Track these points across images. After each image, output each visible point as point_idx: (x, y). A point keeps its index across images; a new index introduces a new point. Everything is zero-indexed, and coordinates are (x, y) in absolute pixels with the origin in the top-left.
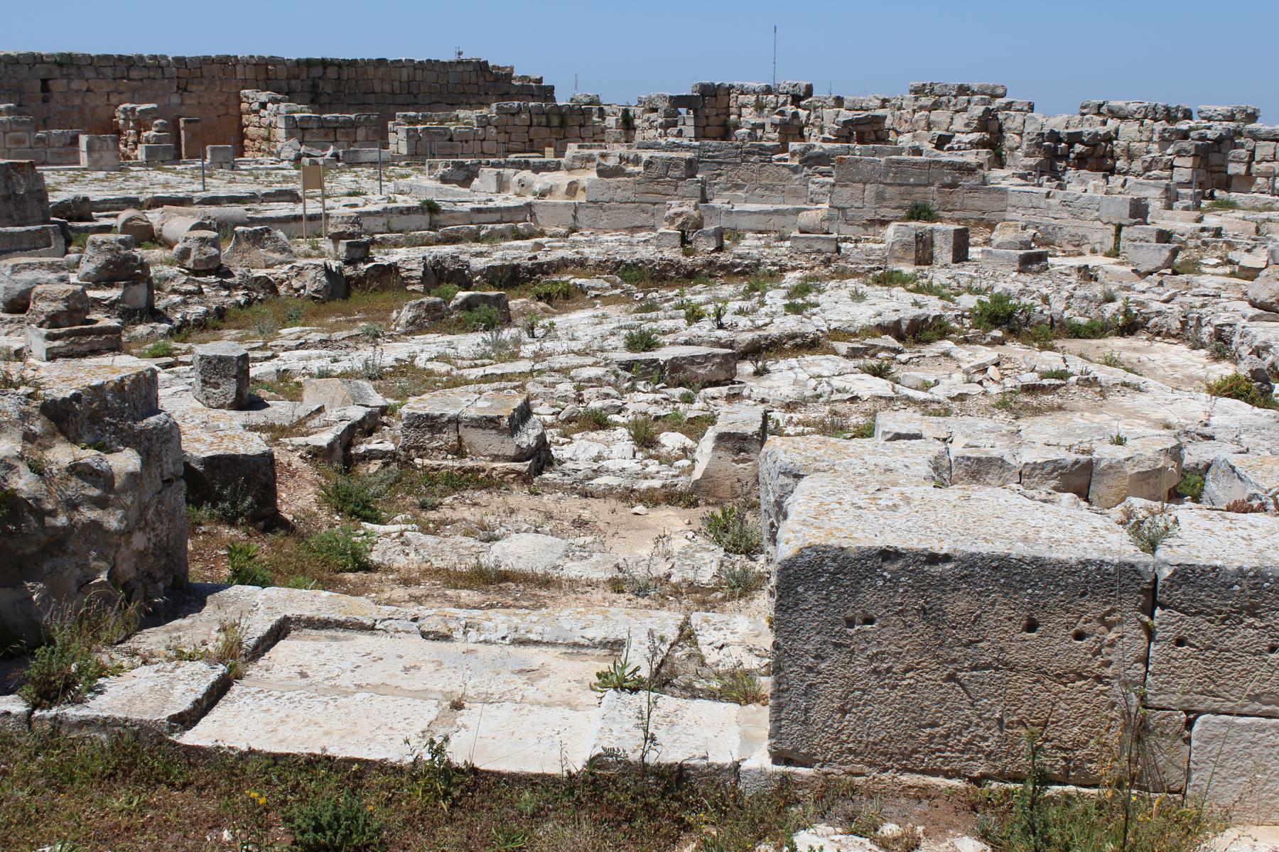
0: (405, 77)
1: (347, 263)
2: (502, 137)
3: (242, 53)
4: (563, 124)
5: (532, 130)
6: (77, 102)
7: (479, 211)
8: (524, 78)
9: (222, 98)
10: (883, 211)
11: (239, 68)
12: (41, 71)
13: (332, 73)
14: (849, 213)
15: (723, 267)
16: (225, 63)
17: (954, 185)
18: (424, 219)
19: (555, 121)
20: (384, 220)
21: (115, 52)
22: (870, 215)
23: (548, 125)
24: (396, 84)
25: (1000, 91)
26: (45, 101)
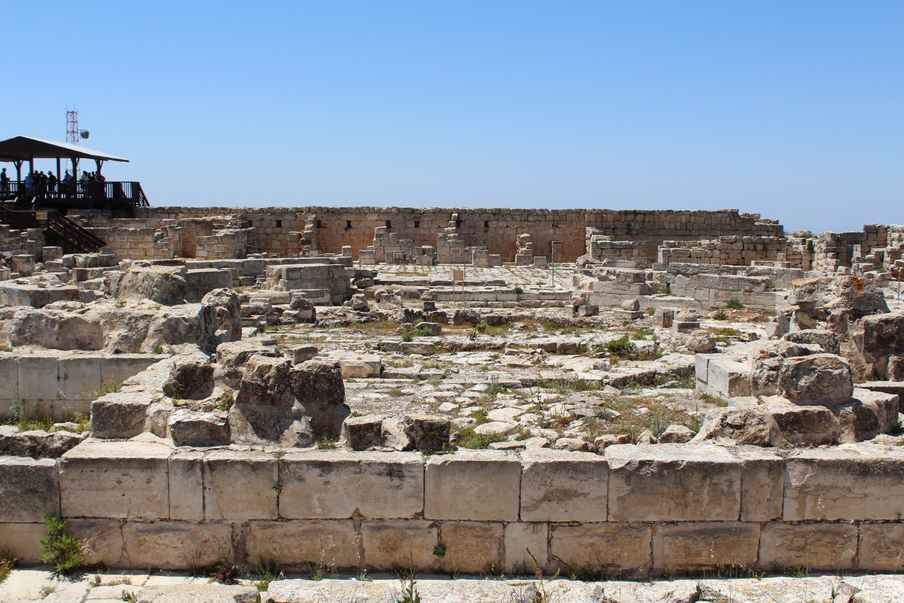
0: (684, 220)
2: (723, 256)
3: (589, 207)
5: (744, 253)
6: (501, 232)
7: (544, 294)
8: (766, 221)
9: (576, 231)
10: (718, 303)
13: (639, 218)
14: (703, 303)
15: (586, 323)
16: (580, 213)
17: (750, 291)
18: (515, 296)
19: (760, 247)
20: (494, 295)
21: (522, 208)
22: (712, 305)
23: (755, 249)
24: (678, 224)
26: (486, 231)
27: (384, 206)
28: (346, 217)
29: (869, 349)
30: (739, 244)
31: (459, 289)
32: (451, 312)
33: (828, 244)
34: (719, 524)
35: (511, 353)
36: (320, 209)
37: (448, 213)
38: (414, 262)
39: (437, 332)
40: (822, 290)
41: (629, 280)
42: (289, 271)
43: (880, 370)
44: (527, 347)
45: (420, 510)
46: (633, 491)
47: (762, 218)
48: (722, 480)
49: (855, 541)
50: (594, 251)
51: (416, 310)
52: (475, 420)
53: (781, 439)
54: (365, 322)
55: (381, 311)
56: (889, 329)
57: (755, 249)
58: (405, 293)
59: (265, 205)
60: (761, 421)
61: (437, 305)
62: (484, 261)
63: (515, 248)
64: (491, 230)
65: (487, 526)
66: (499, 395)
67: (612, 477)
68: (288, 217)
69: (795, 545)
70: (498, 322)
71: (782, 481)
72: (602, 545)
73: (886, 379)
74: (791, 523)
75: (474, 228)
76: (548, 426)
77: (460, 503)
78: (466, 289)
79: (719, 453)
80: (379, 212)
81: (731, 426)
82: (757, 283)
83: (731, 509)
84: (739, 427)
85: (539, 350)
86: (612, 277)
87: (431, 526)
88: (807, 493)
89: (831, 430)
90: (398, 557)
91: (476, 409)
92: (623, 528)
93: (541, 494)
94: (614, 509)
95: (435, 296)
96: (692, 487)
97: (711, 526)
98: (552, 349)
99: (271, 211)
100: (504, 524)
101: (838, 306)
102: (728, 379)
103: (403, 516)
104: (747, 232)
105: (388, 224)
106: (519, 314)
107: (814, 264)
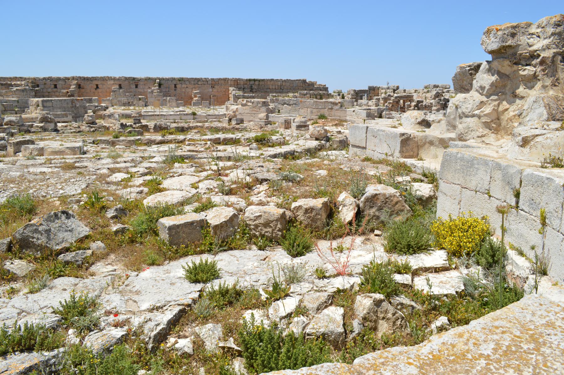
0: (279, 84)
1: (134, 124)
6: (184, 90)
7: (209, 115)
8: (320, 85)
10: (313, 117)
12: (174, 82)
13: (257, 83)
16: (225, 80)
17: (332, 109)
18: (192, 116)
19: (319, 97)
20: (179, 117)
21: (194, 77)
24: (277, 86)
25: (448, 87)
26: (175, 90)
27: (117, 76)
28: (95, 82)
32: (151, 124)
33: (352, 95)
35: (189, 145)
36: (80, 77)
37: (154, 80)
38: (134, 105)
39: (142, 134)
41: (260, 105)
42: (43, 101)
44: (200, 140)
47: (318, 83)
50: (234, 99)
52: (146, 190)
54: (93, 131)
55: (104, 125)
58: (123, 115)
59: (47, 75)
61: (142, 121)
63: (192, 99)
64: (178, 89)
66: (176, 165)
68: (60, 82)
70: (182, 130)
76: (230, 192)
80: (114, 79)
85: (209, 142)
86: (249, 104)
91: (148, 178)
98: (217, 142)
99: (50, 79)
101: (548, 47)
102: (399, 140)
105: (120, 87)
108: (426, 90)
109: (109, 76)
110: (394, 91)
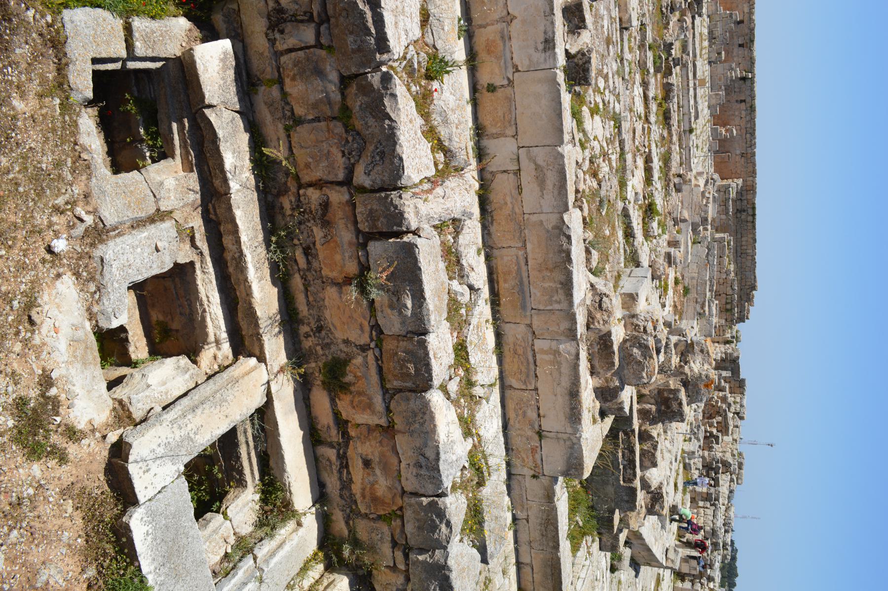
0: (748, 251)
2: (721, 281)
3: (758, 180)
4: (727, 310)
6: (737, 113)
8: (748, 310)
11: (751, 178)
12: (748, 100)
13: (750, 218)
16: (754, 172)
17: (697, 302)
18: (687, 128)
19: (729, 307)
22: (685, 275)
23: (727, 303)
25: (740, 482)
26: (737, 101)
27: (756, 17)
29: (660, 392)
30: (730, 292)
31: (691, 84)
32: (674, 79)
33: (731, 354)
34: (528, 294)
35: (643, 129)
37: (751, 70)
38: (710, 46)
39: (657, 70)
40: (704, 359)
41: (703, 214)
43: (645, 399)
44: (649, 141)
45: (520, 69)
46: (548, 231)
47: (751, 308)
48: (561, 296)
49: (524, 387)
50: (723, 186)
51: (673, 52)
52: (592, 106)
53: (593, 336)
54: (662, 11)
55: (671, 23)
56: (675, 406)
57: (727, 303)
58: (686, 41)
60: (605, 322)
61: (678, 68)
62: (714, 102)
63: (724, 125)
64: (738, 105)
65: (513, 123)
66: (612, 123)
67: (557, 216)
69: (518, 347)
71: (562, 338)
72: (507, 211)
73: (638, 403)
74: (533, 345)
75: (740, 92)
76: (591, 162)
77: (528, 99)
78: (691, 90)
79: (581, 293)
80: (751, 13)
81: (601, 301)
82: (703, 307)
83: (540, 303)
84: (600, 306)
85: (647, 150)
86: (704, 202)
87: (508, 79)
88: (555, 355)
89: (601, 371)
90: (482, 55)
91: (601, 106)
92: (520, 227)
93: (540, 162)
94: (534, 218)
95: (685, 66)
96: (554, 274)
97: (526, 289)
98: (648, 160)
100: (515, 136)
101: (692, 370)
102: (633, 292)
103: (514, 56)
104: (740, 297)
105: (741, 22)
106: (674, 133)
107: (716, 344)
108: (735, 452)
109: (755, 6)
110: (738, 414)
